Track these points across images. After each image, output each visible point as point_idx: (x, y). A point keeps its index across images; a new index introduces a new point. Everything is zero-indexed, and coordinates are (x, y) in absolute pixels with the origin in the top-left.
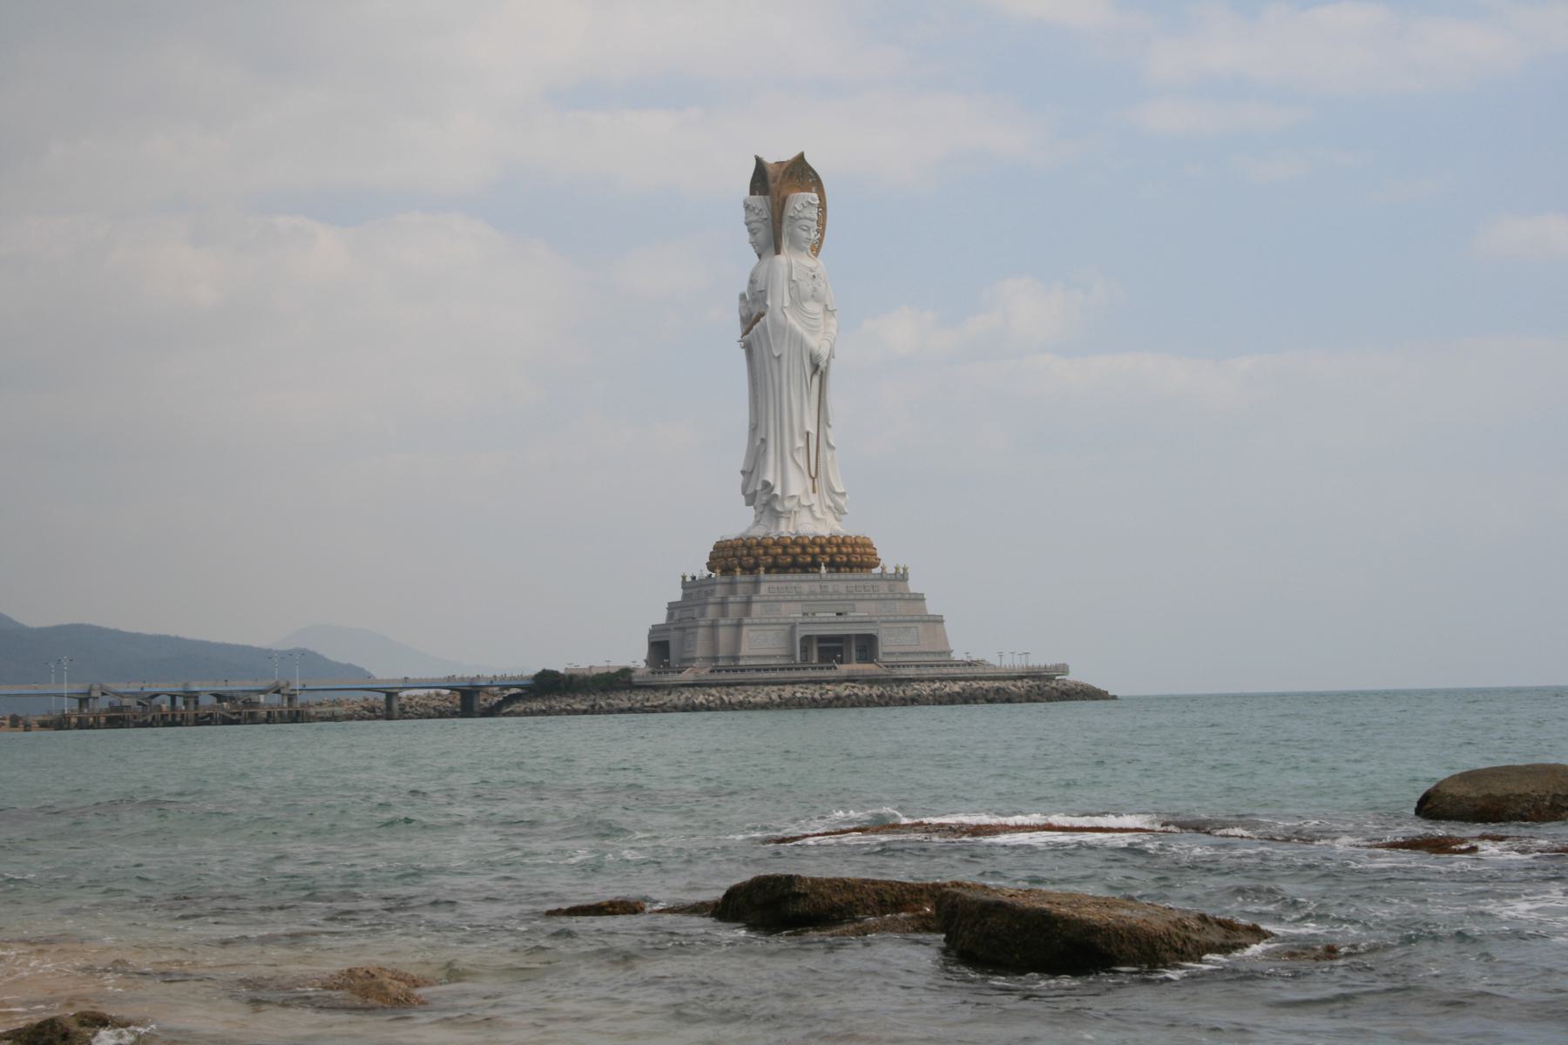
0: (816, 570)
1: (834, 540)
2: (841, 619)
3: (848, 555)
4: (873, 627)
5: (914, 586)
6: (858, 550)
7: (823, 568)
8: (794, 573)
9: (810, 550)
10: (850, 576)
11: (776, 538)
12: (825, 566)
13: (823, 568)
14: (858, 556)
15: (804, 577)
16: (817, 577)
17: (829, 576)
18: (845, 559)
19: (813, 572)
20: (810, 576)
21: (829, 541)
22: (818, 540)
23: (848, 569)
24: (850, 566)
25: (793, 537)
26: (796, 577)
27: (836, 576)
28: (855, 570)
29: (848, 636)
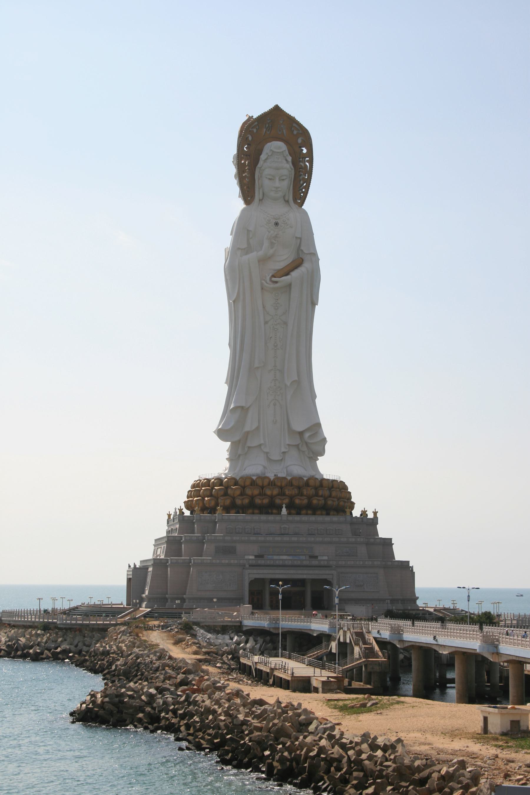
0: (274, 511)
1: (311, 483)
2: (261, 562)
3: (326, 499)
4: (327, 572)
5: (383, 532)
6: (334, 494)
7: (284, 511)
8: (253, 513)
9: (268, 492)
10: (313, 518)
11: (272, 478)
12: (286, 507)
13: (284, 511)
14: (336, 500)
15: (264, 517)
16: (278, 518)
17: (291, 518)
18: (305, 501)
19: (272, 513)
20: (271, 518)
21: (307, 484)
22: (295, 483)
23: (324, 512)
24: (327, 510)
25: (289, 478)
26: (256, 517)
27: (297, 518)
28: (332, 513)
29: (302, 582)
